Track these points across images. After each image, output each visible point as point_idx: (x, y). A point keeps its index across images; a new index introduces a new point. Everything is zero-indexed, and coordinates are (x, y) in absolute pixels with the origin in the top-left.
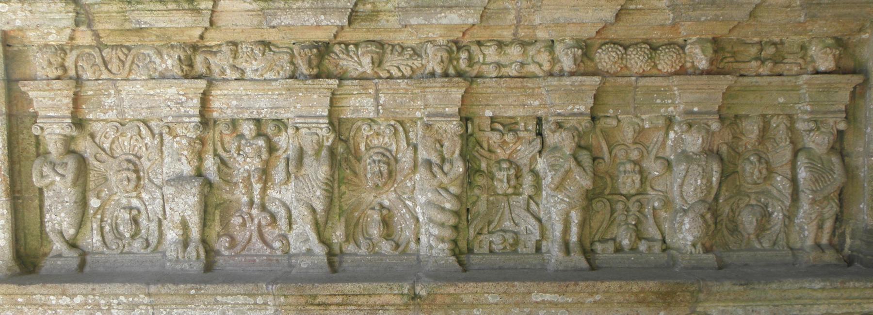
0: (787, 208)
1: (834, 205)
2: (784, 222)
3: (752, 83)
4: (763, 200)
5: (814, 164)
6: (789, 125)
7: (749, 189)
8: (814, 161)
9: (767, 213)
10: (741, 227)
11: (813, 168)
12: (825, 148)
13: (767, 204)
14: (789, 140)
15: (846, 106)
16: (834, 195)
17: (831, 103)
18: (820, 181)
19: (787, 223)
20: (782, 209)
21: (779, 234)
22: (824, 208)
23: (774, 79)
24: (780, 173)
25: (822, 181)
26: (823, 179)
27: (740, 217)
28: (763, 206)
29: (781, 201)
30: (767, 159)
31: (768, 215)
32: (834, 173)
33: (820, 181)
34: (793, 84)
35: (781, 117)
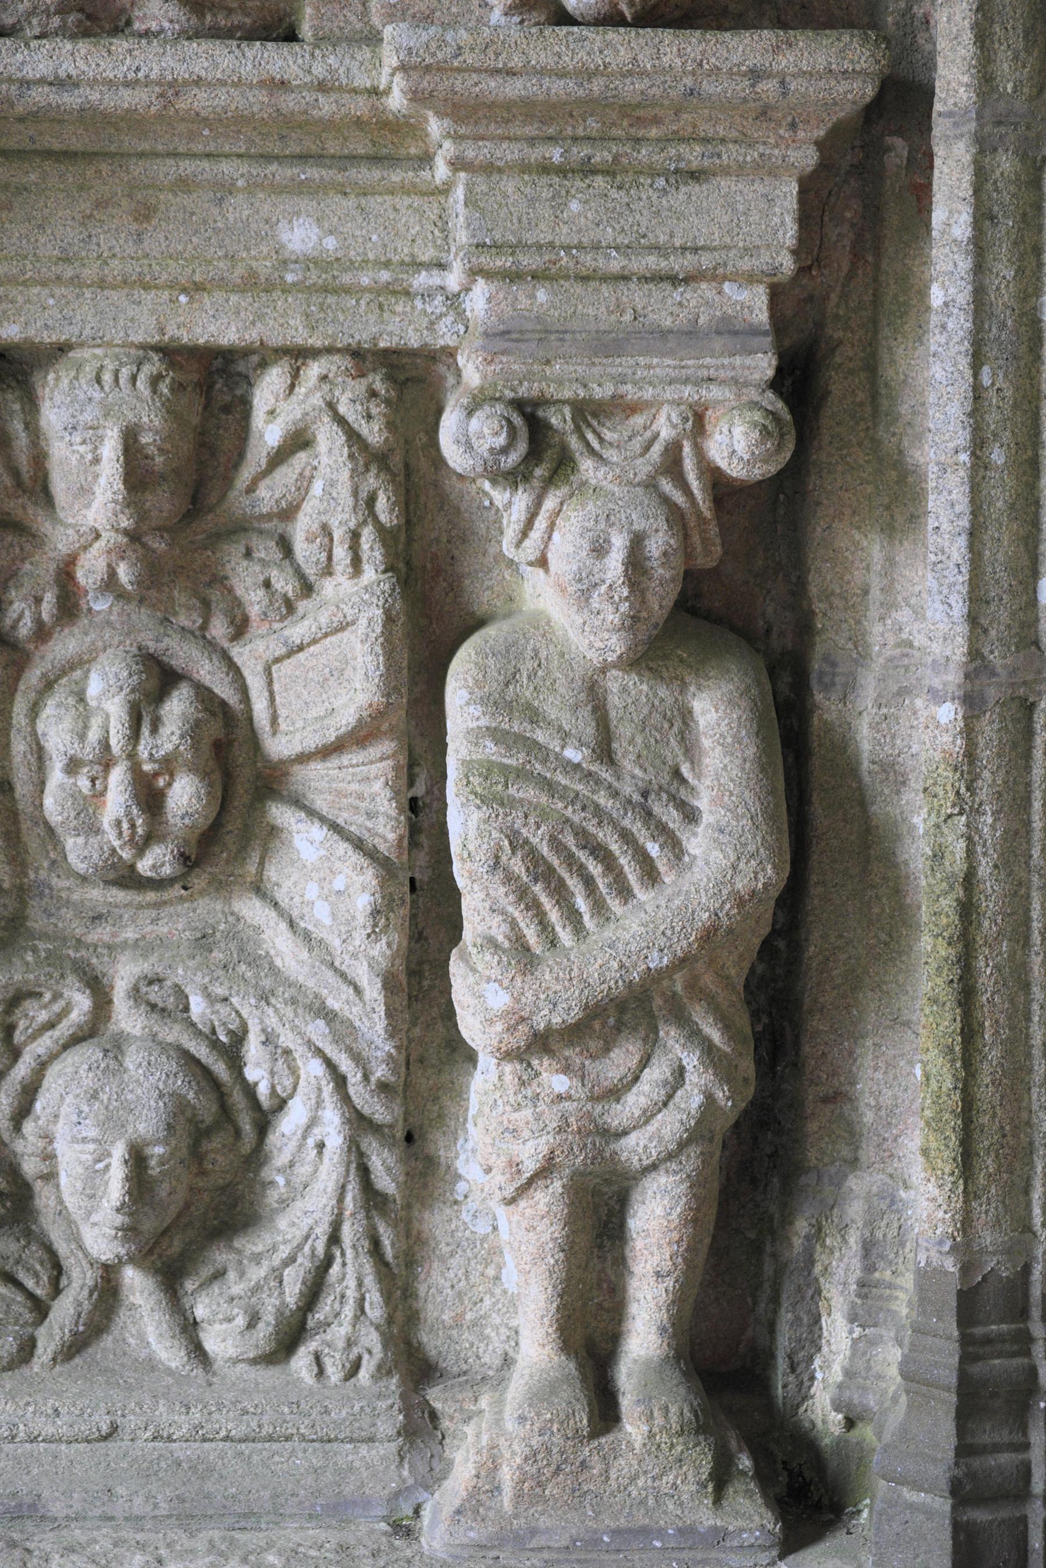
0: (380, 1072)
1: (691, 1060)
2: (364, 1171)
3: (26, 84)
4: (198, 1006)
5: (533, 747)
6: (374, 433)
7: (97, 918)
8: (534, 716)
9: (237, 1098)
10: (44, 1198)
11: (521, 774)
12: (612, 617)
13: (239, 1037)
14: (378, 555)
15: (775, 294)
16: (693, 985)
17: (652, 262)
18: (573, 883)
19: (385, 1182)
20: (340, 1081)
21: (328, 1262)
22: (615, 1093)
23: (200, 67)
24: (321, 803)
25: (589, 882)
26: (595, 869)
27: (29, 1127)
28: (202, 1051)
29: (329, 1016)
30: (224, 690)
31: (247, 1127)
32: (691, 816)
33: (573, 883)
34: (360, 106)
35: (314, 370)
